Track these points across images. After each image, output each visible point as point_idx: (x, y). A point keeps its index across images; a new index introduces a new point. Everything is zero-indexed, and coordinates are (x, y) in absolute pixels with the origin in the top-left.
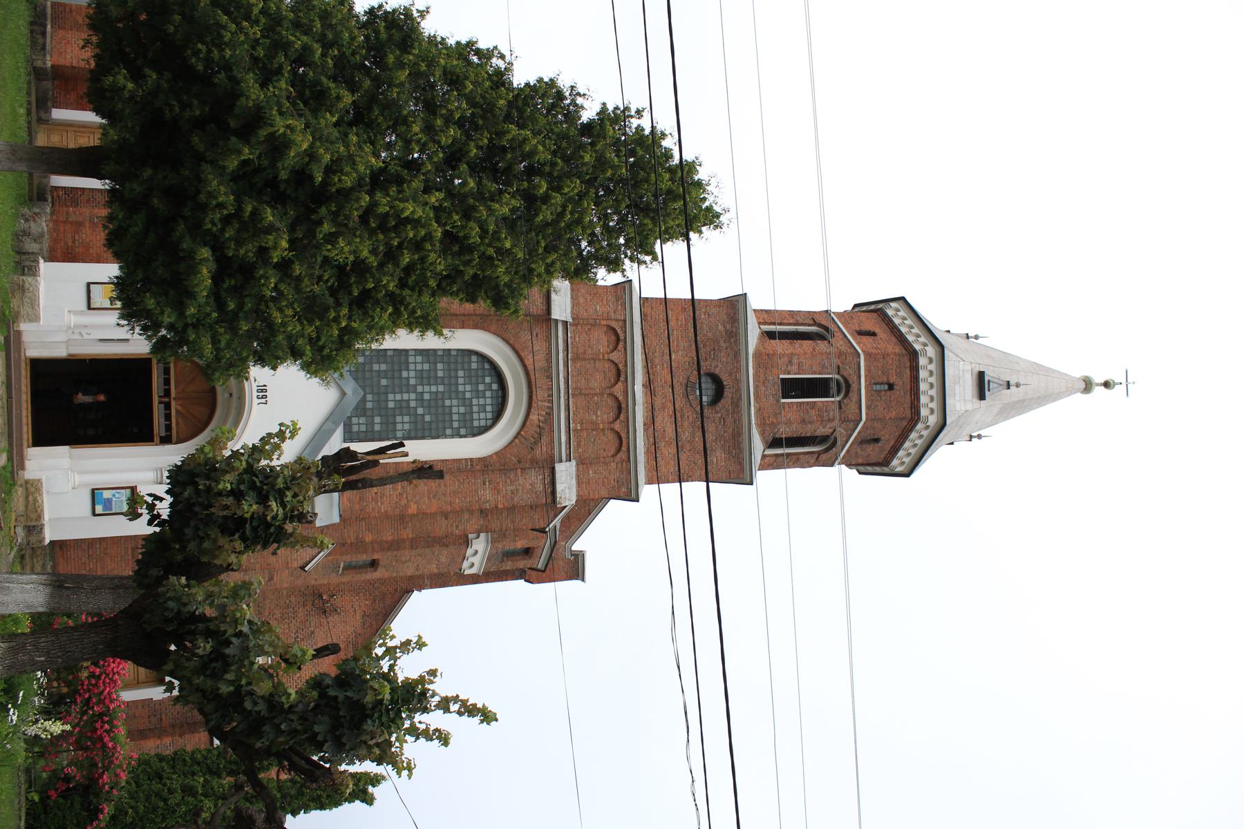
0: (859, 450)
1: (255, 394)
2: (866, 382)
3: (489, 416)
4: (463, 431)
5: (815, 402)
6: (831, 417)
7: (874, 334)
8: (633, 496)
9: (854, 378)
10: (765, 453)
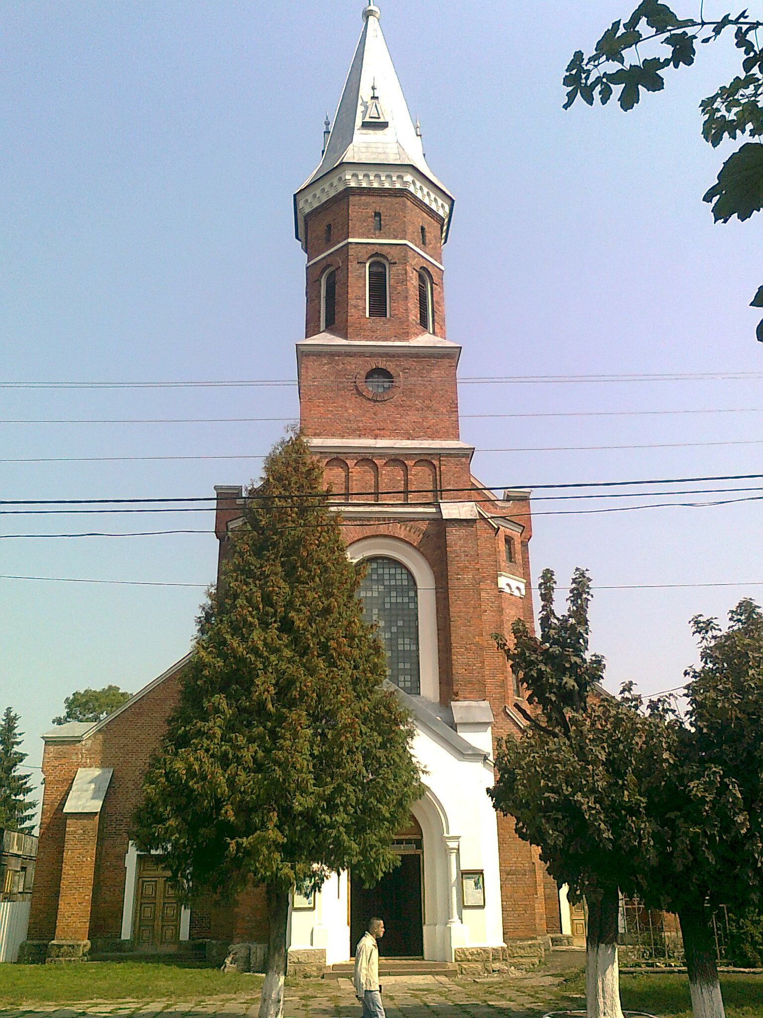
0: (431, 246)
2: (372, 238)
3: (399, 571)
4: (412, 594)
6: (404, 272)
7: (329, 226)
8: (470, 452)
10: (431, 332)
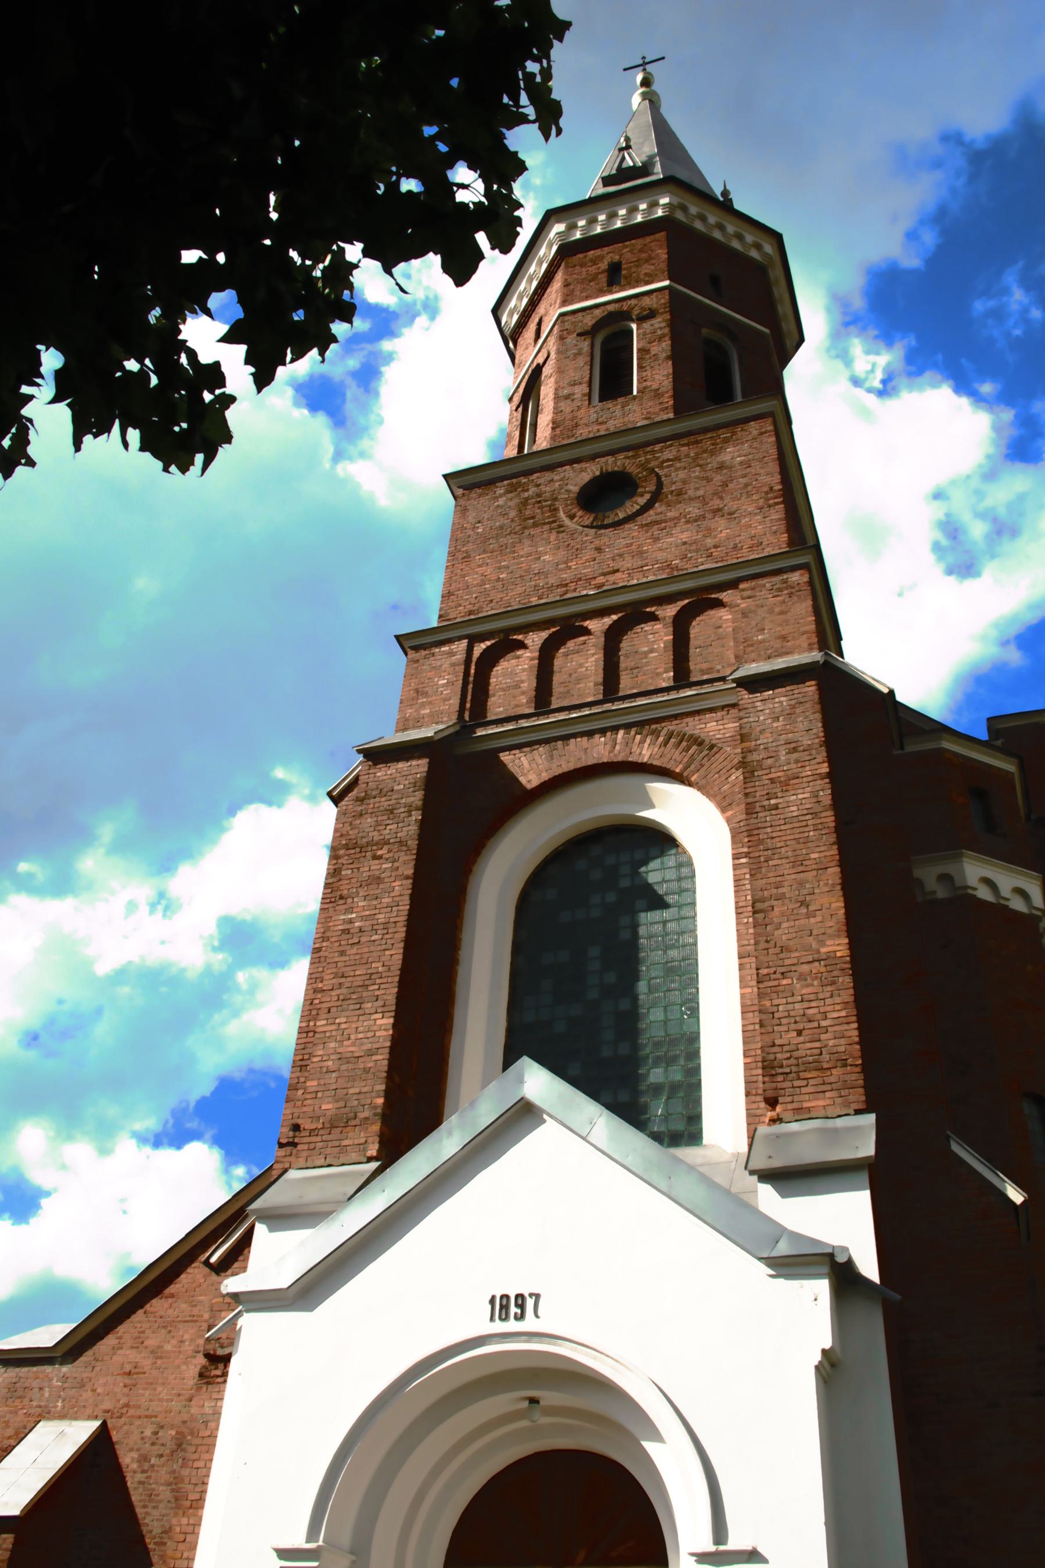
1: (512, 1326)
5: (639, 350)
9: (598, 313)
